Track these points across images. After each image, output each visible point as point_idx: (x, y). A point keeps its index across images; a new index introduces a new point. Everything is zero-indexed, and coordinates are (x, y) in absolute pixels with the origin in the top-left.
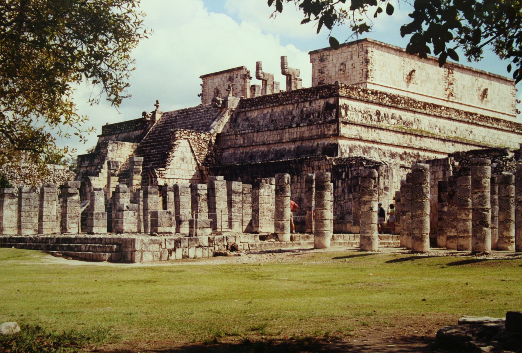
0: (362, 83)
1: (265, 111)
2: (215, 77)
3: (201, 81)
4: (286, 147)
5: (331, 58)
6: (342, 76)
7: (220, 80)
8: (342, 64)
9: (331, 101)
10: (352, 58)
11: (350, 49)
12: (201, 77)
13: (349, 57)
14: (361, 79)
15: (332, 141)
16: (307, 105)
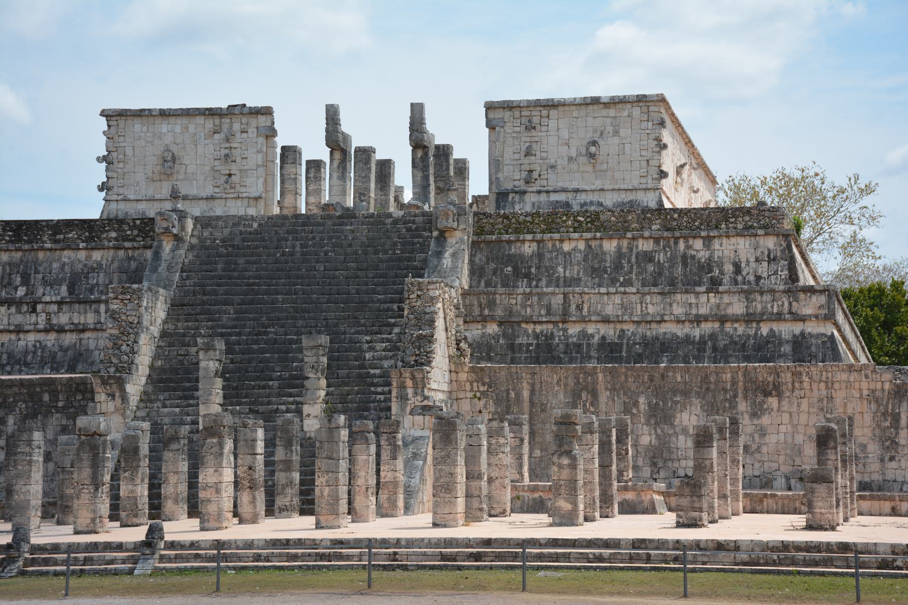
0: (646, 189)
1: (567, 247)
2: (158, 120)
3: (103, 123)
4: (680, 331)
5: (553, 124)
6: (589, 168)
7: (178, 129)
8: (594, 143)
10: (616, 133)
11: (612, 112)
12: (103, 113)
13: (610, 129)
14: (643, 180)
15: (812, 328)
16: (698, 244)
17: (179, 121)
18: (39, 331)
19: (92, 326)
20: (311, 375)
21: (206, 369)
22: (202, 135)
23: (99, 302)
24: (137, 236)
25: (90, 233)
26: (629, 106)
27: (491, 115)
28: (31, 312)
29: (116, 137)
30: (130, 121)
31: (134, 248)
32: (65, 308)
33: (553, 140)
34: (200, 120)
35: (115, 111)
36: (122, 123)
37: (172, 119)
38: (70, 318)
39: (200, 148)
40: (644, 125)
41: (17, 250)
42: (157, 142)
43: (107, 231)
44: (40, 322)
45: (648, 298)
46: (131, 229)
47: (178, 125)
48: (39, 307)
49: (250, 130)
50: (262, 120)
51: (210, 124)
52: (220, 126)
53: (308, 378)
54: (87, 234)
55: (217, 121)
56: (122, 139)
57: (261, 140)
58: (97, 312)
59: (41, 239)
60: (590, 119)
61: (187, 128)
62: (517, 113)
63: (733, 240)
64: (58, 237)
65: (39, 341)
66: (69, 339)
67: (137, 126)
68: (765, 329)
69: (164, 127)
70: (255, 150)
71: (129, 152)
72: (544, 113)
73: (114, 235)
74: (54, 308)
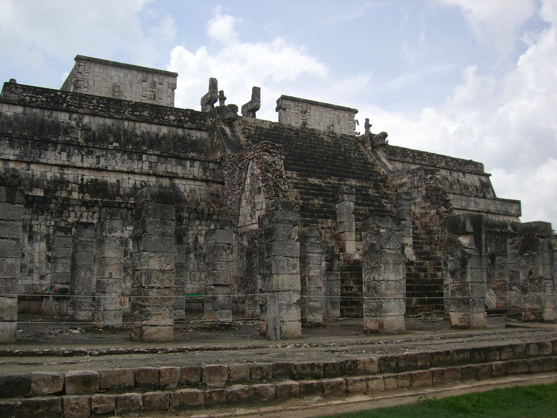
7: (122, 75)
9: (484, 179)
11: (337, 113)
17: (122, 71)
18: (142, 174)
19: (181, 175)
20: (408, 218)
21: (349, 208)
22: (136, 81)
23: (187, 159)
24: (188, 121)
25: (157, 114)
26: (343, 112)
27: (284, 102)
28: (138, 160)
29: (83, 72)
30: (92, 65)
31: (190, 129)
32: (162, 159)
33: (313, 121)
34: (135, 73)
35: (86, 57)
36: (88, 64)
37: (118, 69)
38: (166, 168)
39: (134, 89)
40: (350, 122)
41: (110, 117)
42: (109, 80)
43: (169, 115)
44: (144, 168)
45: (463, 197)
46: (185, 116)
47: (122, 73)
48: (144, 157)
49: (164, 84)
50: (171, 79)
51: (140, 76)
52: (147, 77)
53: (406, 220)
54: (155, 114)
55: (145, 75)
56: (87, 74)
57: (170, 90)
58: (184, 166)
59: (124, 113)
60: (328, 114)
61: (127, 75)
62: (297, 103)
63: (472, 175)
64: (136, 113)
65: (144, 182)
66: (166, 182)
67: (97, 69)
68: (501, 218)
69: (113, 72)
70: (166, 95)
71: (91, 83)
72: (309, 106)
73: (172, 118)
74: (154, 159)
